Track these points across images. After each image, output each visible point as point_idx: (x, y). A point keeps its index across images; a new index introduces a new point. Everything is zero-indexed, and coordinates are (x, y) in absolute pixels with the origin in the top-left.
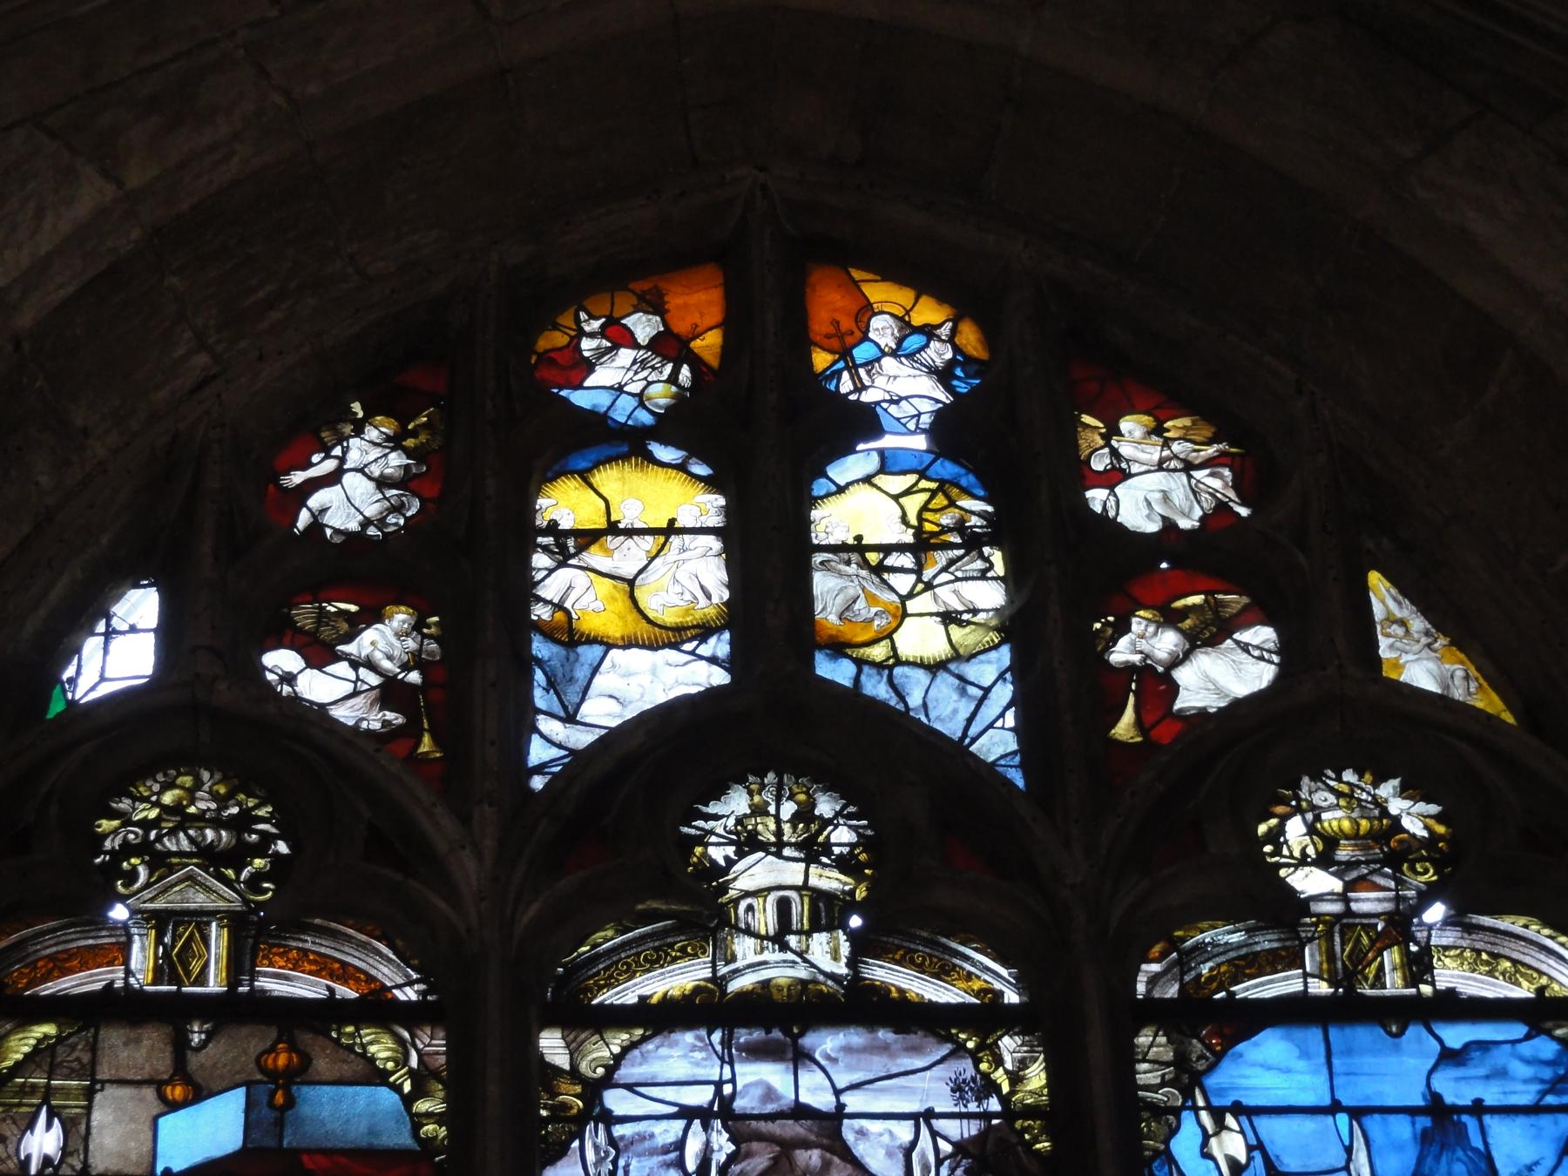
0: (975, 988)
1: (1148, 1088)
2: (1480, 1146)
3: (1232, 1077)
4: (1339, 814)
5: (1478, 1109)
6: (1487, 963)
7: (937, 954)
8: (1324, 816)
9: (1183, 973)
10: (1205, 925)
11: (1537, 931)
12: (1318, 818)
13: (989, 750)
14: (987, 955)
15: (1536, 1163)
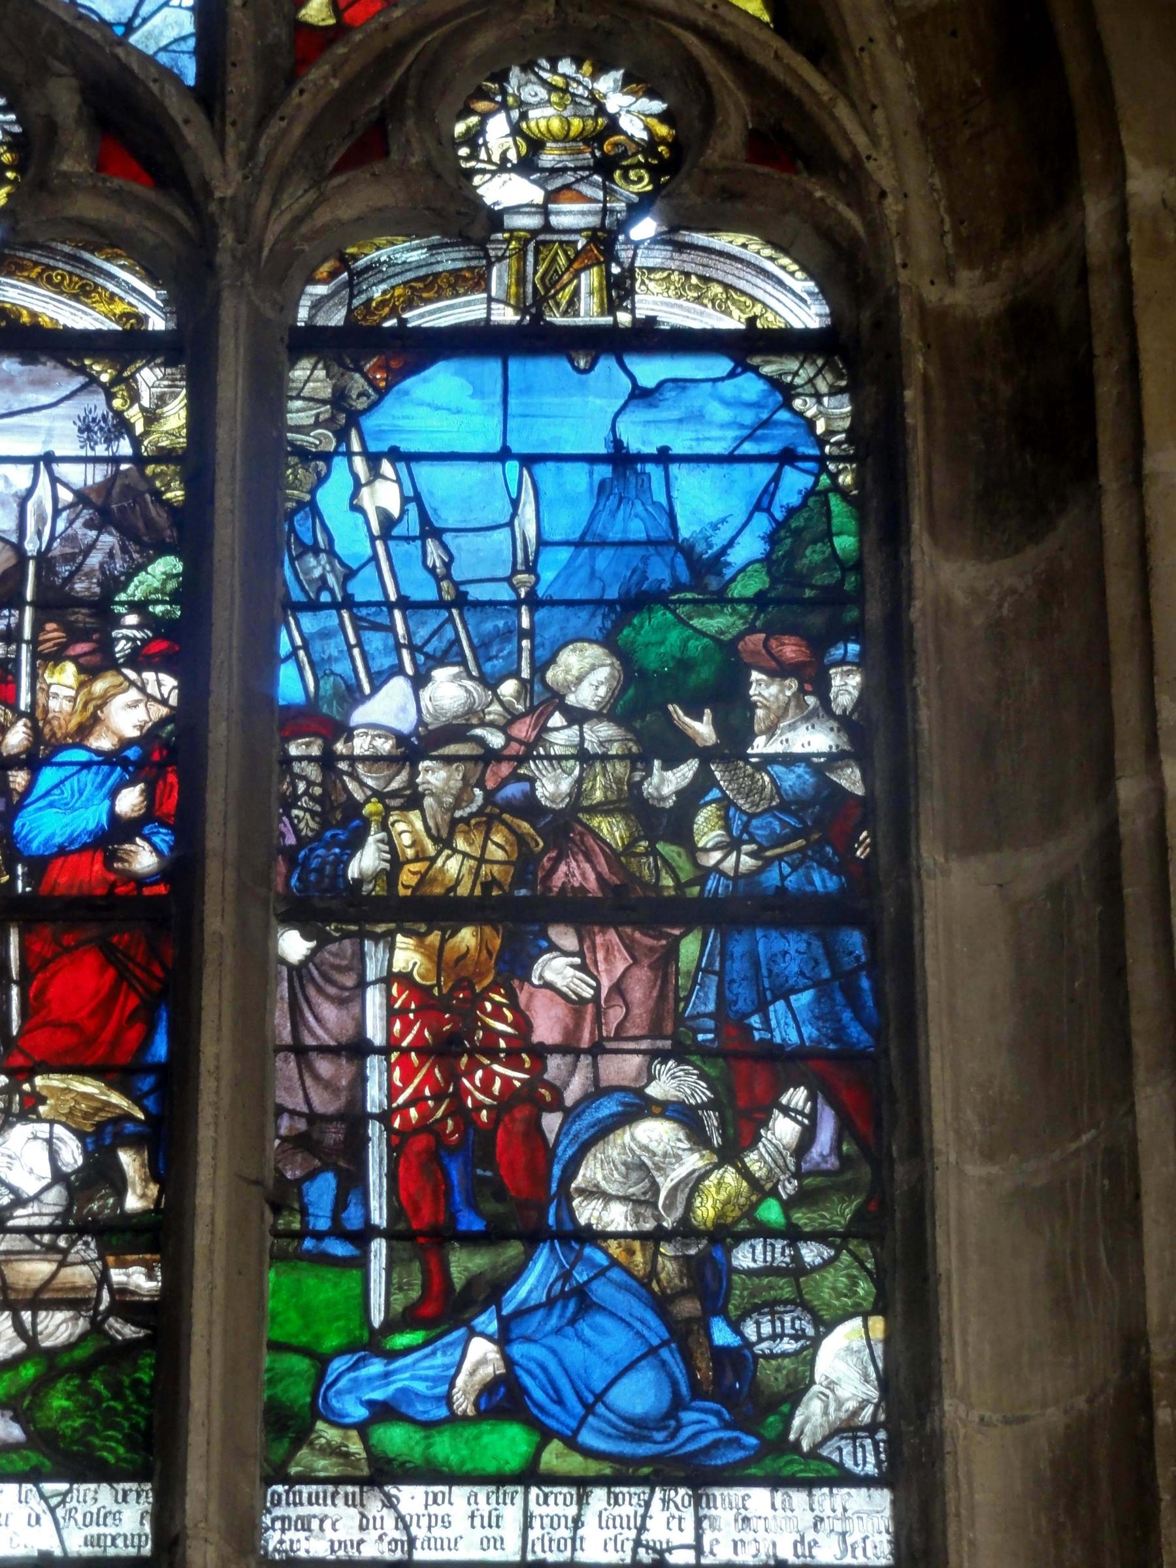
0: (118, 312)
1: (298, 429)
2: (663, 500)
3: (394, 417)
4: (549, 111)
5: (664, 457)
6: (697, 287)
7: (78, 271)
8: (532, 114)
9: (352, 296)
10: (381, 240)
11: (754, 249)
12: (524, 116)
13: (161, 33)
14: (134, 273)
15: (724, 521)
